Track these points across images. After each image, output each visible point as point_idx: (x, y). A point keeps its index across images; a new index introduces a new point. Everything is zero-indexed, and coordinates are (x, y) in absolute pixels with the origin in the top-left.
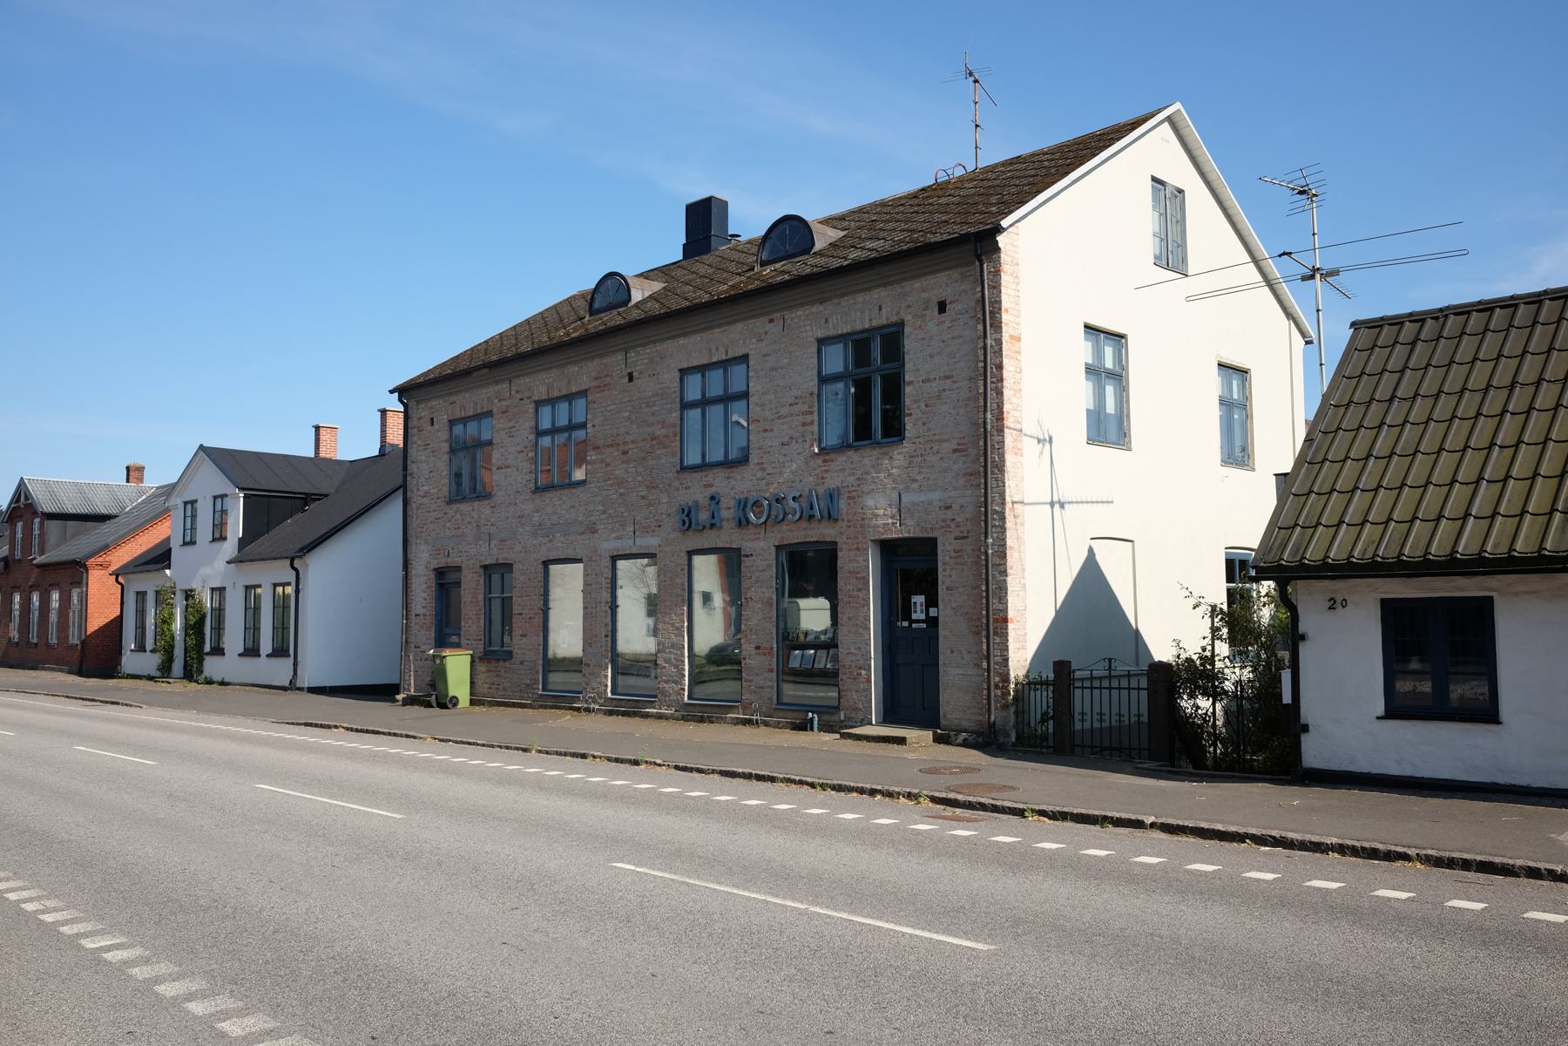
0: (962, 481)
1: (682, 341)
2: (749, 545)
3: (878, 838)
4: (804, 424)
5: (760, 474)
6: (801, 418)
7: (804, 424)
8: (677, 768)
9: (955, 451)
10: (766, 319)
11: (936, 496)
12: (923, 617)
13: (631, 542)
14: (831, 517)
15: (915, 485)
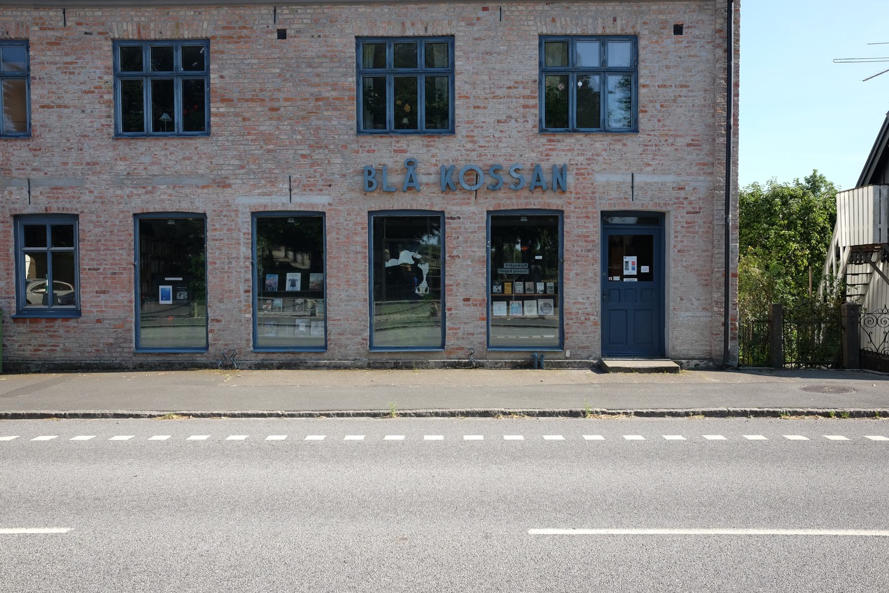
0: (695, 169)
1: (362, 9)
2: (455, 208)
3: (596, 453)
4: (525, 107)
5: (469, 146)
6: (522, 101)
7: (525, 107)
8: (638, 414)
9: (689, 145)
10: (479, 6)
11: (670, 179)
12: (635, 273)
13: (285, 199)
14: (560, 187)
15: (649, 169)
